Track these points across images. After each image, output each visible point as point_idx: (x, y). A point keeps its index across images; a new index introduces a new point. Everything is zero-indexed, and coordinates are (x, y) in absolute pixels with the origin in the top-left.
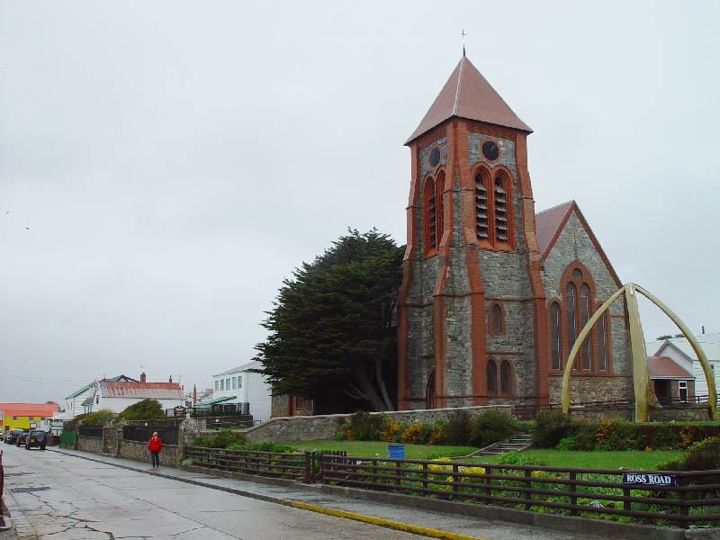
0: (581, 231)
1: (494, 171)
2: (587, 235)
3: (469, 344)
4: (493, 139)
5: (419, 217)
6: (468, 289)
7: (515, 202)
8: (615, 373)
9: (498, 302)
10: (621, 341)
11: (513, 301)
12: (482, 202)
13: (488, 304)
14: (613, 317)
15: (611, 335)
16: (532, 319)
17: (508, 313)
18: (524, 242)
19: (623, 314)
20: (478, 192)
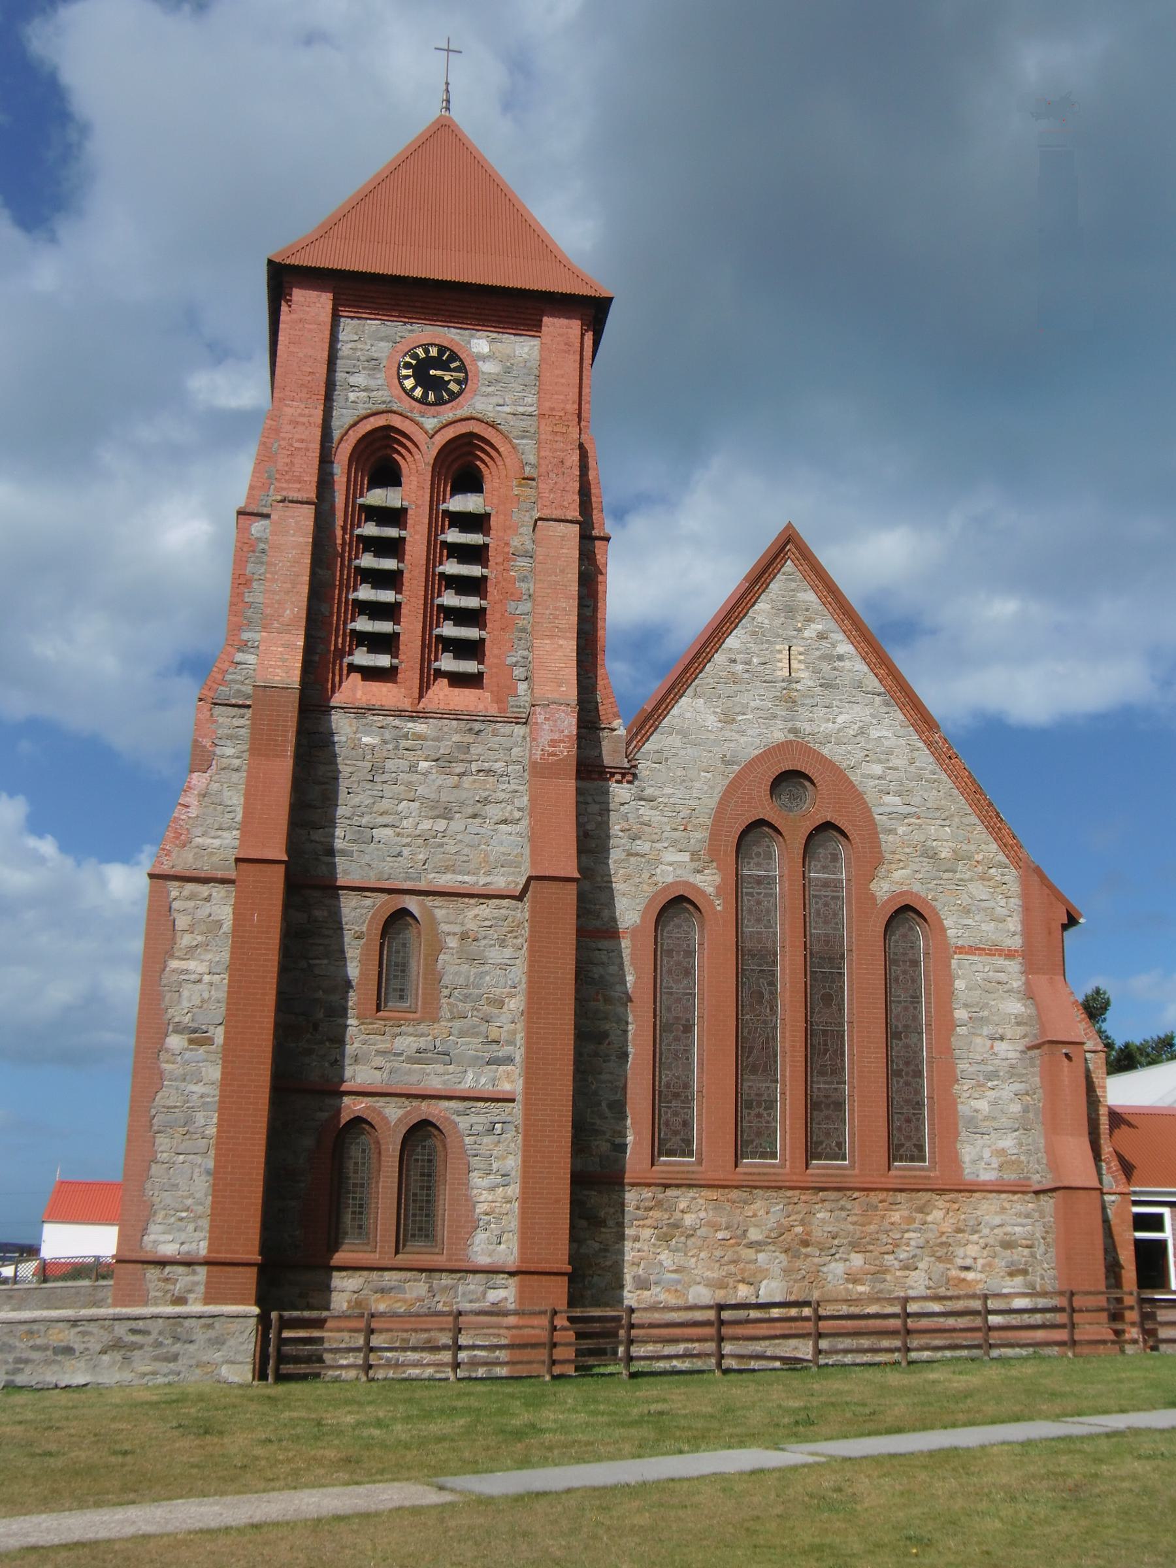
0: (821, 636)
4: (450, 335)
9: (412, 904)
14: (960, 950)
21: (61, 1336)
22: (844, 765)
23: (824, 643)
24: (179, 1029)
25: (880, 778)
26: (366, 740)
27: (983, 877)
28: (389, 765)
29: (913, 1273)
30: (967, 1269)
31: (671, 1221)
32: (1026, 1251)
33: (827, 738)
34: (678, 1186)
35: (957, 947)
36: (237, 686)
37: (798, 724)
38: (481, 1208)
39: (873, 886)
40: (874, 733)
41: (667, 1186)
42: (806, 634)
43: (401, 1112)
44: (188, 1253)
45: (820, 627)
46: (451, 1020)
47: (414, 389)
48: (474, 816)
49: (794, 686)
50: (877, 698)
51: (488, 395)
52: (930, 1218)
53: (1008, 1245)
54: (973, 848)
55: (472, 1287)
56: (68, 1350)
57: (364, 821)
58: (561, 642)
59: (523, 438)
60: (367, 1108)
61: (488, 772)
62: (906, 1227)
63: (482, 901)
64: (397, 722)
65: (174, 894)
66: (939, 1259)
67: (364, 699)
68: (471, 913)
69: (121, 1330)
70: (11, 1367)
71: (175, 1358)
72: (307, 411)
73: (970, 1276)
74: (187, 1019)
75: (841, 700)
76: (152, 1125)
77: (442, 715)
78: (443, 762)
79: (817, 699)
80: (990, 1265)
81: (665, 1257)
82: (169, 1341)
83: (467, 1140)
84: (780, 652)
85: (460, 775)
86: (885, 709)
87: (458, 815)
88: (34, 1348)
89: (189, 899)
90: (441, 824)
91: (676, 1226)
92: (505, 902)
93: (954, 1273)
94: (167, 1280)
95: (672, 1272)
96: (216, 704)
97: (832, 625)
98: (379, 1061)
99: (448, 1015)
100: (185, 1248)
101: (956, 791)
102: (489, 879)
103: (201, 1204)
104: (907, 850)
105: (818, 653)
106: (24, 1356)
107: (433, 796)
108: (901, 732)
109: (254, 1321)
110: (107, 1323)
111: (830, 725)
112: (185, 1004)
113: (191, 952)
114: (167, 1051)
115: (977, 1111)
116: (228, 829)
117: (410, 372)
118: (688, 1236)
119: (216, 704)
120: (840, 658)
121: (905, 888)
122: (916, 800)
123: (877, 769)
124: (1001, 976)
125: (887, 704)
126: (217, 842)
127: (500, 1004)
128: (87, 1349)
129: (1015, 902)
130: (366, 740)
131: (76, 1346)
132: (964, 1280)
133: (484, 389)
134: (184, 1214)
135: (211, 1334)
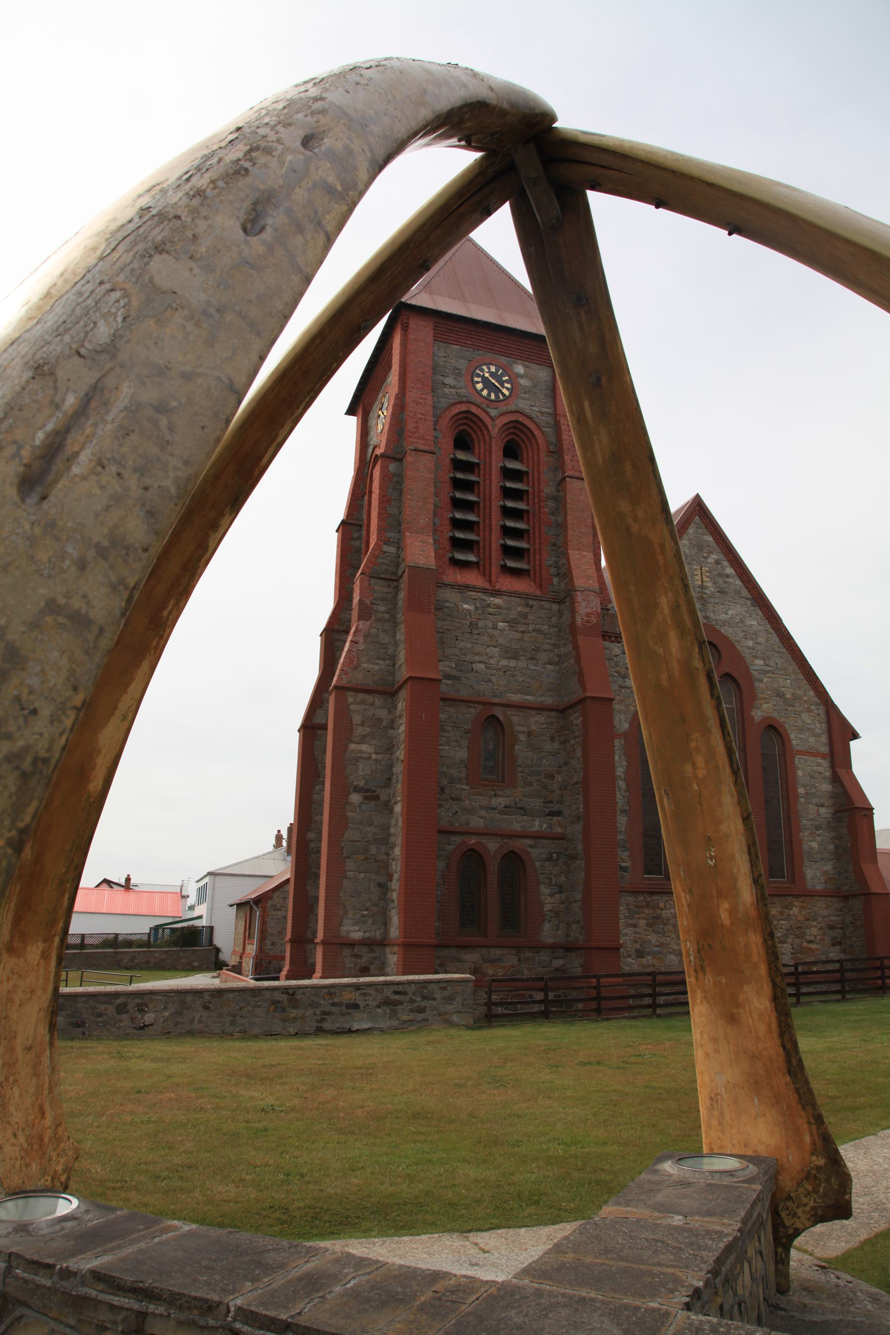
0: (717, 562)
1: (500, 422)
2: (729, 570)
3: (398, 808)
5: (355, 543)
6: (403, 673)
7: (548, 490)
8: (809, 886)
9: (499, 713)
10: (823, 810)
11: (540, 709)
12: (468, 486)
13: (467, 715)
14: (800, 752)
15: (797, 797)
16: (579, 753)
17: (523, 738)
18: (566, 574)
19: (825, 749)
20: (458, 465)
21: (350, 996)
22: (733, 640)
23: (719, 566)
24: (357, 790)
25: (753, 649)
26: (465, 606)
27: (809, 710)
28: (481, 624)
29: (785, 945)
30: (810, 942)
31: (655, 915)
32: (840, 931)
33: (724, 623)
34: (658, 893)
35: (797, 751)
36: (384, 567)
37: (708, 614)
38: (547, 907)
39: (753, 713)
40: (748, 622)
41: (652, 893)
42: (709, 560)
43: (497, 845)
44: (369, 938)
45: (716, 557)
46: (523, 787)
47: (482, 390)
48: (532, 659)
49: (704, 591)
50: (749, 602)
51: (525, 399)
52: (791, 912)
53: (831, 927)
54: (802, 693)
55: (543, 958)
56: (356, 1006)
57: (467, 658)
58: (584, 553)
59: (547, 427)
60: (478, 843)
61: (538, 631)
62: (779, 917)
63: (539, 712)
64: (484, 597)
65: (351, 700)
66: (797, 937)
67: (463, 581)
68: (533, 720)
69: (388, 992)
70: (318, 1017)
71: (422, 1010)
72: (423, 396)
73: (813, 946)
74: (362, 783)
75: (729, 601)
76: (342, 854)
77: (511, 594)
78: (513, 623)
79: (717, 600)
80: (822, 939)
81: (653, 938)
82: (419, 999)
83: (537, 864)
84: (696, 570)
85: (523, 632)
86: (752, 608)
87: (522, 658)
88: (333, 1004)
89: (359, 703)
90: (513, 663)
91: (657, 918)
92: (553, 714)
93: (805, 944)
94: (357, 956)
95: (656, 946)
96: (372, 577)
97: (722, 556)
98: (483, 813)
99: (523, 784)
100: (367, 935)
101: (791, 660)
102: (543, 699)
103: (377, 906)
104: (769, 692)
105: (715, 572)
106: (327, 1010)
107: (507, 645)
108: (762, 623)
109: (472, 984)
110: (379, 987)
111: (725, 616)
112: (361, 773)
113: (363, 739)
114: (350, 804)
115: (812, 848)
116: (384, 659)
117: (479, 379)
118: (665, 924)
119: (372, 577)
120: (728, 576)
121: (769, 715)
122: (772, 663)
123: (750, 643)
124: (821, 769)
125: (753, 605)
126: (376, 667)
127: (551, 777)
128: (368, 1005)
129: (824, 725)
130: (465, 606)
131: (360, 1003)
132: (810, 948)
133: (523, 395)
134: (366, 913)
135: (446, 993)
